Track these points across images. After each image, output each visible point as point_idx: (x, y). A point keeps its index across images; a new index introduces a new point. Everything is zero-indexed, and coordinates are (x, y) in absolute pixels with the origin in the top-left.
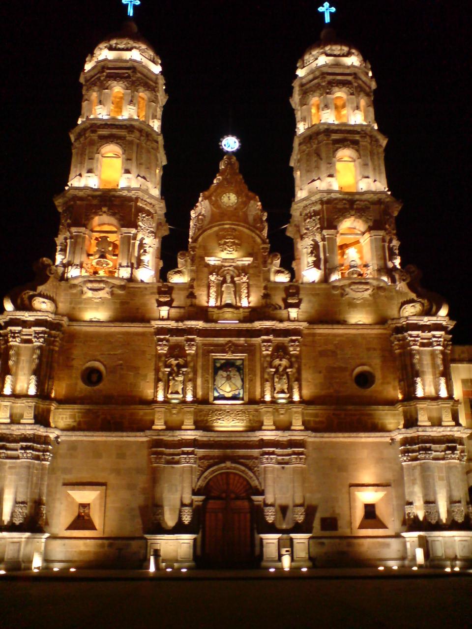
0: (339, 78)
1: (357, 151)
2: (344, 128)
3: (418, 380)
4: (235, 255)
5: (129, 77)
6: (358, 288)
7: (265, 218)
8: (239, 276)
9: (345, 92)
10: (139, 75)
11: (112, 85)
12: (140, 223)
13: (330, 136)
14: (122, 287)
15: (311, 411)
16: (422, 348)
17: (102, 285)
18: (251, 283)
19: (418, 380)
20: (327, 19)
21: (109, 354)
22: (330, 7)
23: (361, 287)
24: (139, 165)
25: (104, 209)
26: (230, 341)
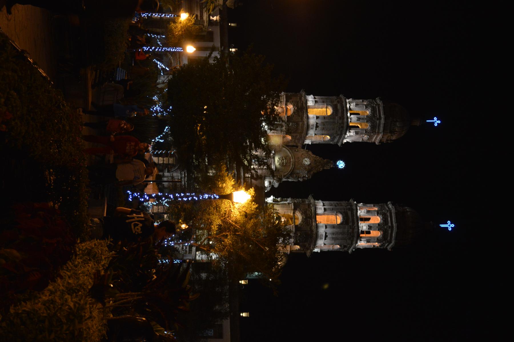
0: (389, 219)
2: (355, 220)
4: (277, 163)
5: (374, 116)
7: (300, 179)
10: (378, 122)
13: (349, 210)
20: (442, 226)
22: (451, 227)
24: (323, 124)
25: (296, 108)
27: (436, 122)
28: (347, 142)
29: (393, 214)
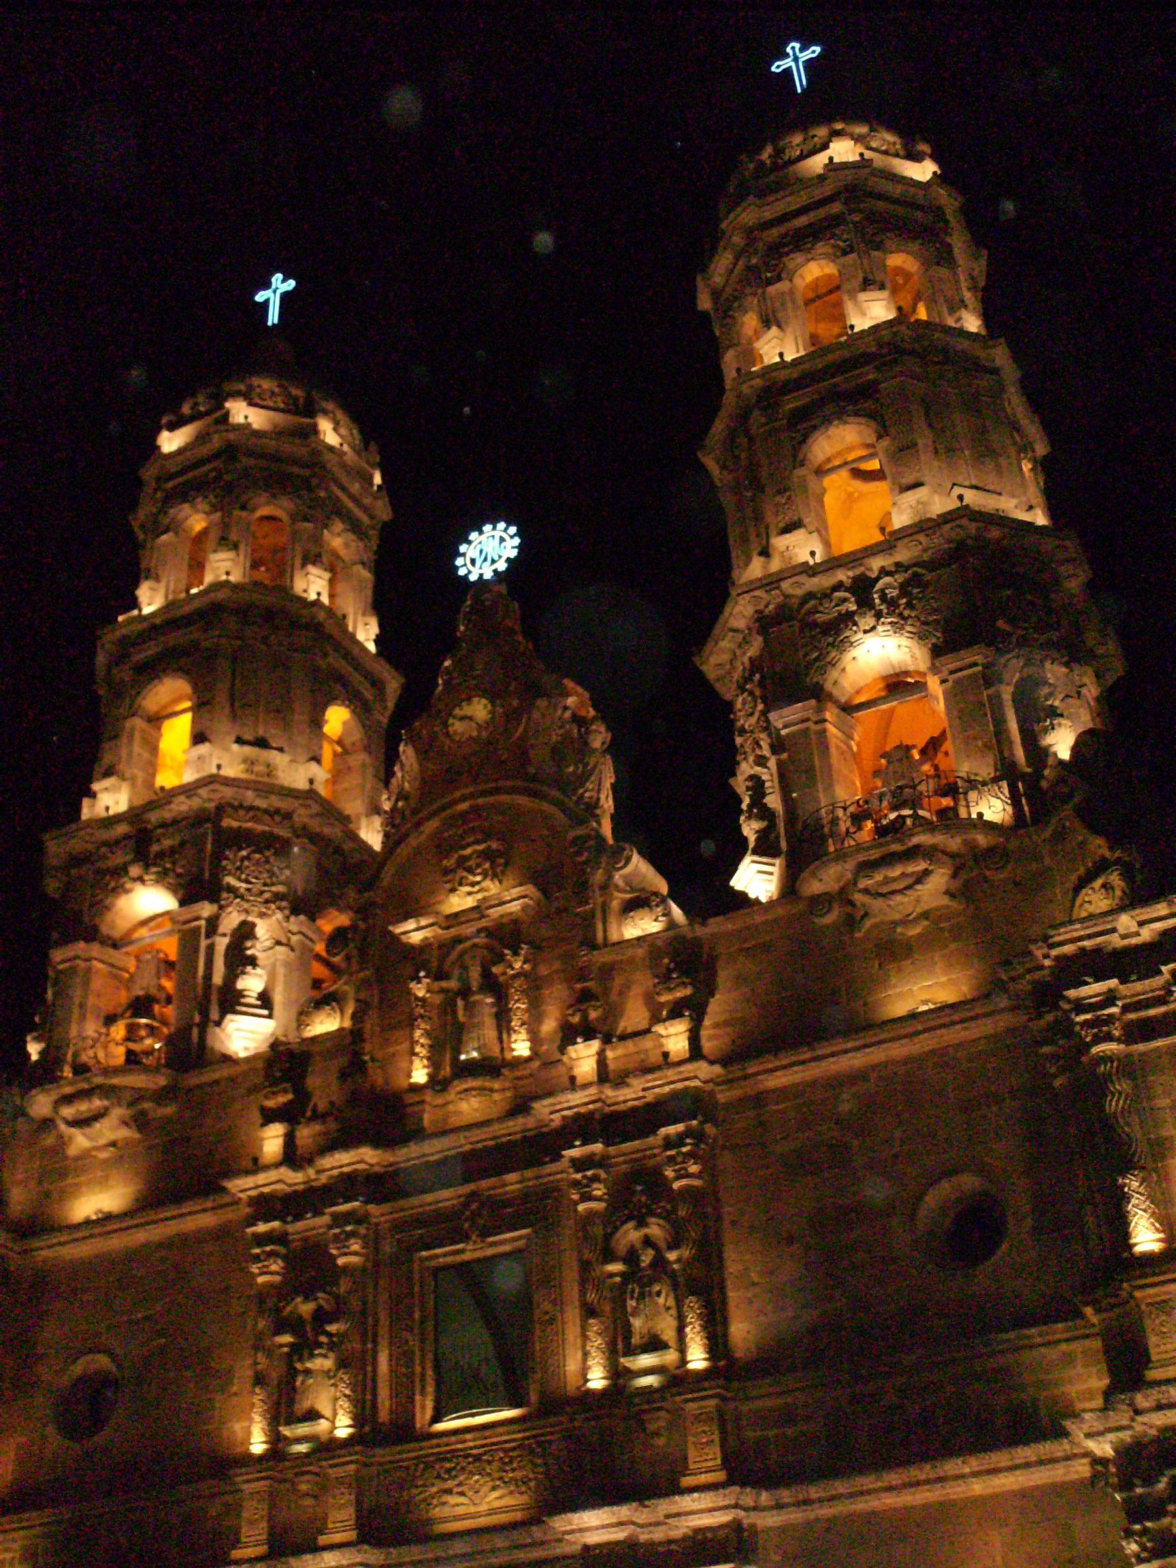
0: (802, 221)
1: (872, 415)
3: (1132, 1183)
6: (887, 880)
8: (501, 958)
9: (826, 256)
10: (246, 461)
11: (181, 516)
12: (230, 880)
13: (777, 404)
14: (161, 1096)
15: (768, 1403)
16: (1141, 1047)
17: (98, 1103)
18: (544, 970)
19: (1132, 1183)
21: (130, 1322)
23: (896, 872)
26: (474, 1194)
27: (276, 290)
28: (378, 641)
29: (768, 214)
